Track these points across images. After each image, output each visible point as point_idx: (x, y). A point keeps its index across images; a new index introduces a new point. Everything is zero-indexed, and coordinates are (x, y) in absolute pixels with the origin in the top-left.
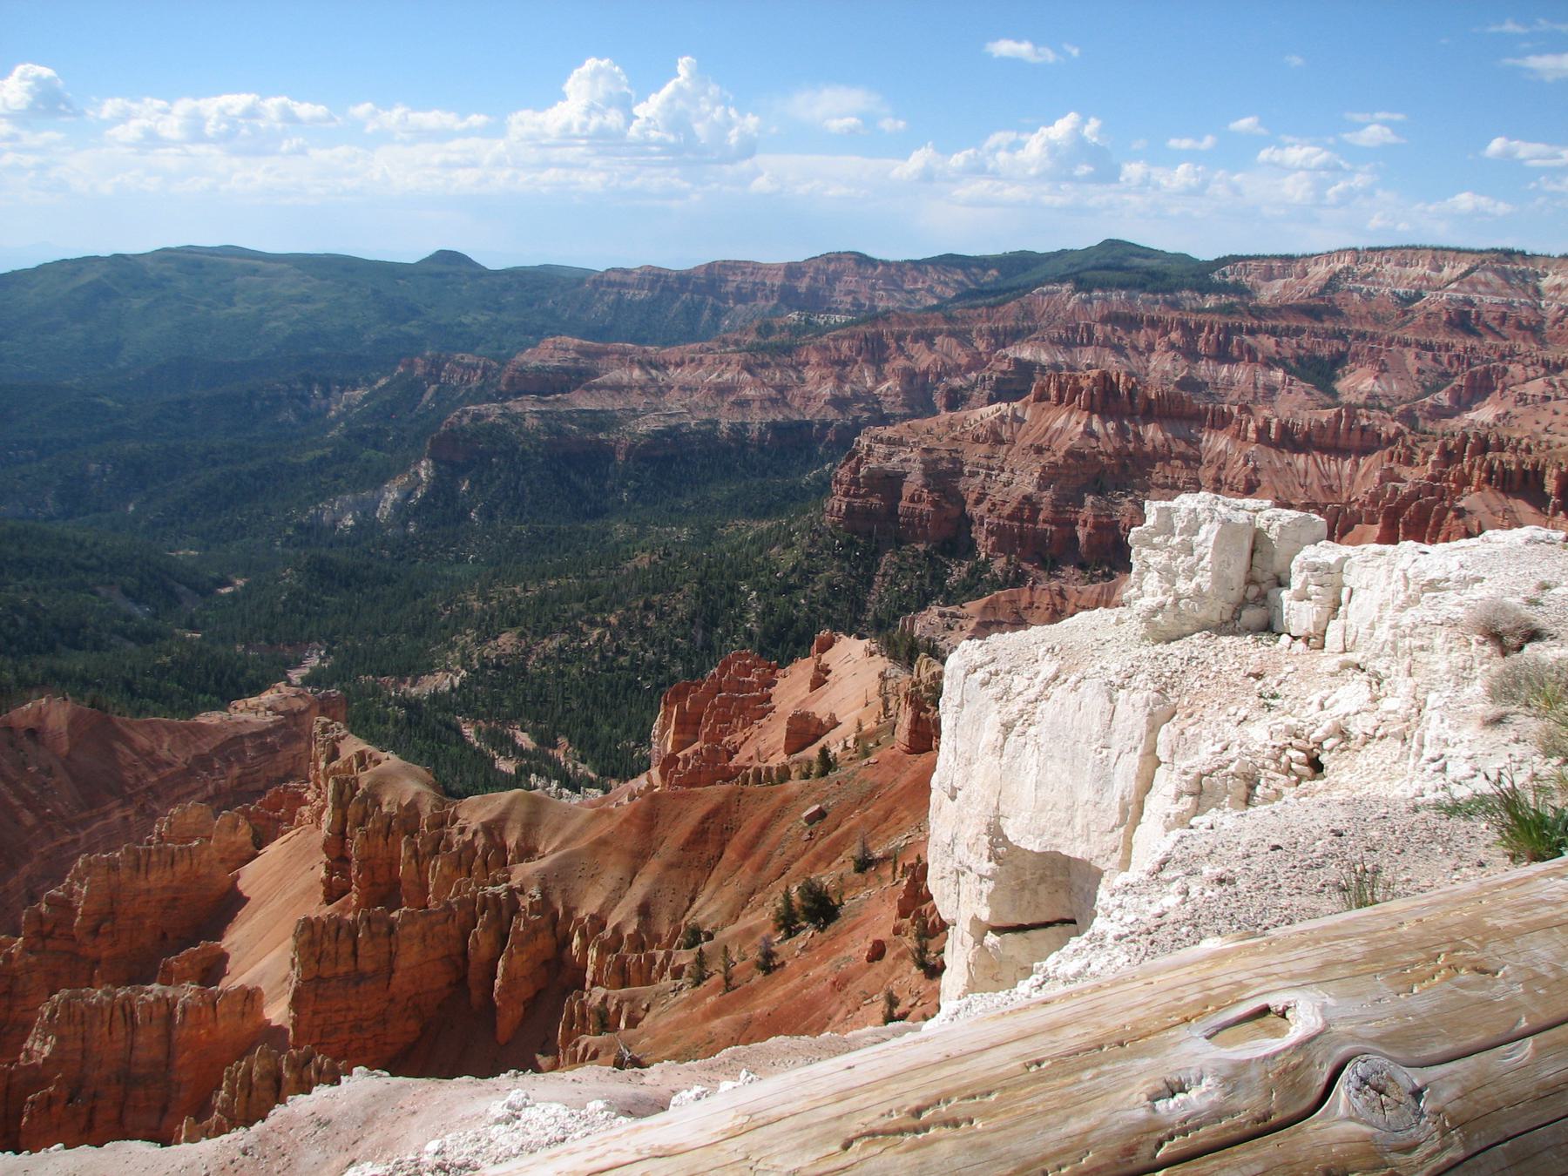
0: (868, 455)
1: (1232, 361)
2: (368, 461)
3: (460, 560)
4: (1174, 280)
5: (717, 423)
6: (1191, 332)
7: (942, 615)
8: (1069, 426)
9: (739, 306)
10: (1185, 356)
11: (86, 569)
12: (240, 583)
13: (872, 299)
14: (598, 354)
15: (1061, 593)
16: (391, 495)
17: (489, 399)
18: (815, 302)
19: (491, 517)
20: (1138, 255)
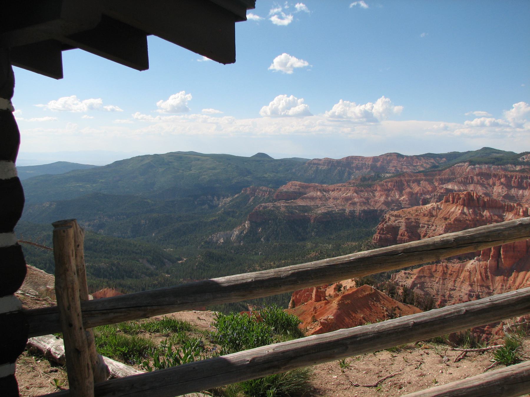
0: (389, 220)
1: (524, 189)
2: (230, 221)
3: (256, 254)
4: (505, 161)
5: (345, 210)
6: (509, 179)
7: (405, 273)
8: (456, 210)
9: (357, 171)
10: (506, 187)
11: (136, 253)
12: (185, 259)
13: (401, 169)
14: (307, 187)
15: (446, 267)
16: (236, 232)
17: (270, 202)
18: (383, 169)
19: (268, 240)
20: (495, 153)
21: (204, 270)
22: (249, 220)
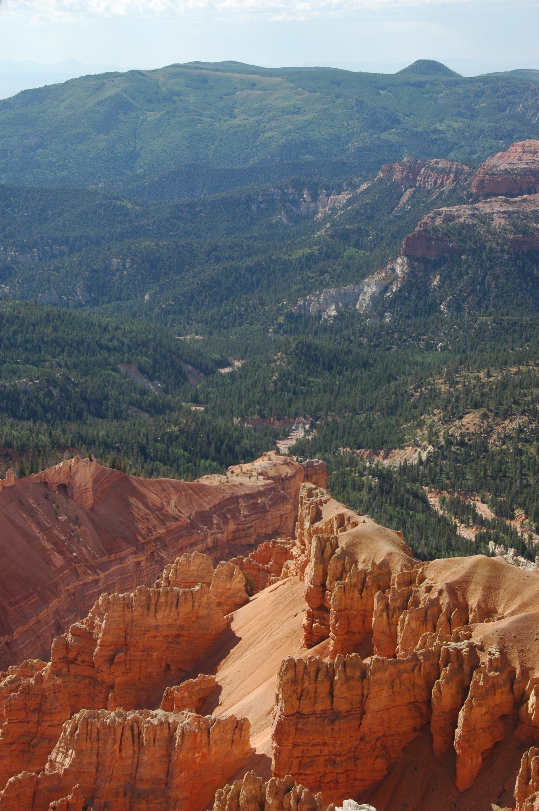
2: (350, 258)
11: (109, 350)
12: (238, 364)
16: (370, 288)
17: (461, 201)
19: (459, 309)
21: (295, 393)
22: (405, 255)
